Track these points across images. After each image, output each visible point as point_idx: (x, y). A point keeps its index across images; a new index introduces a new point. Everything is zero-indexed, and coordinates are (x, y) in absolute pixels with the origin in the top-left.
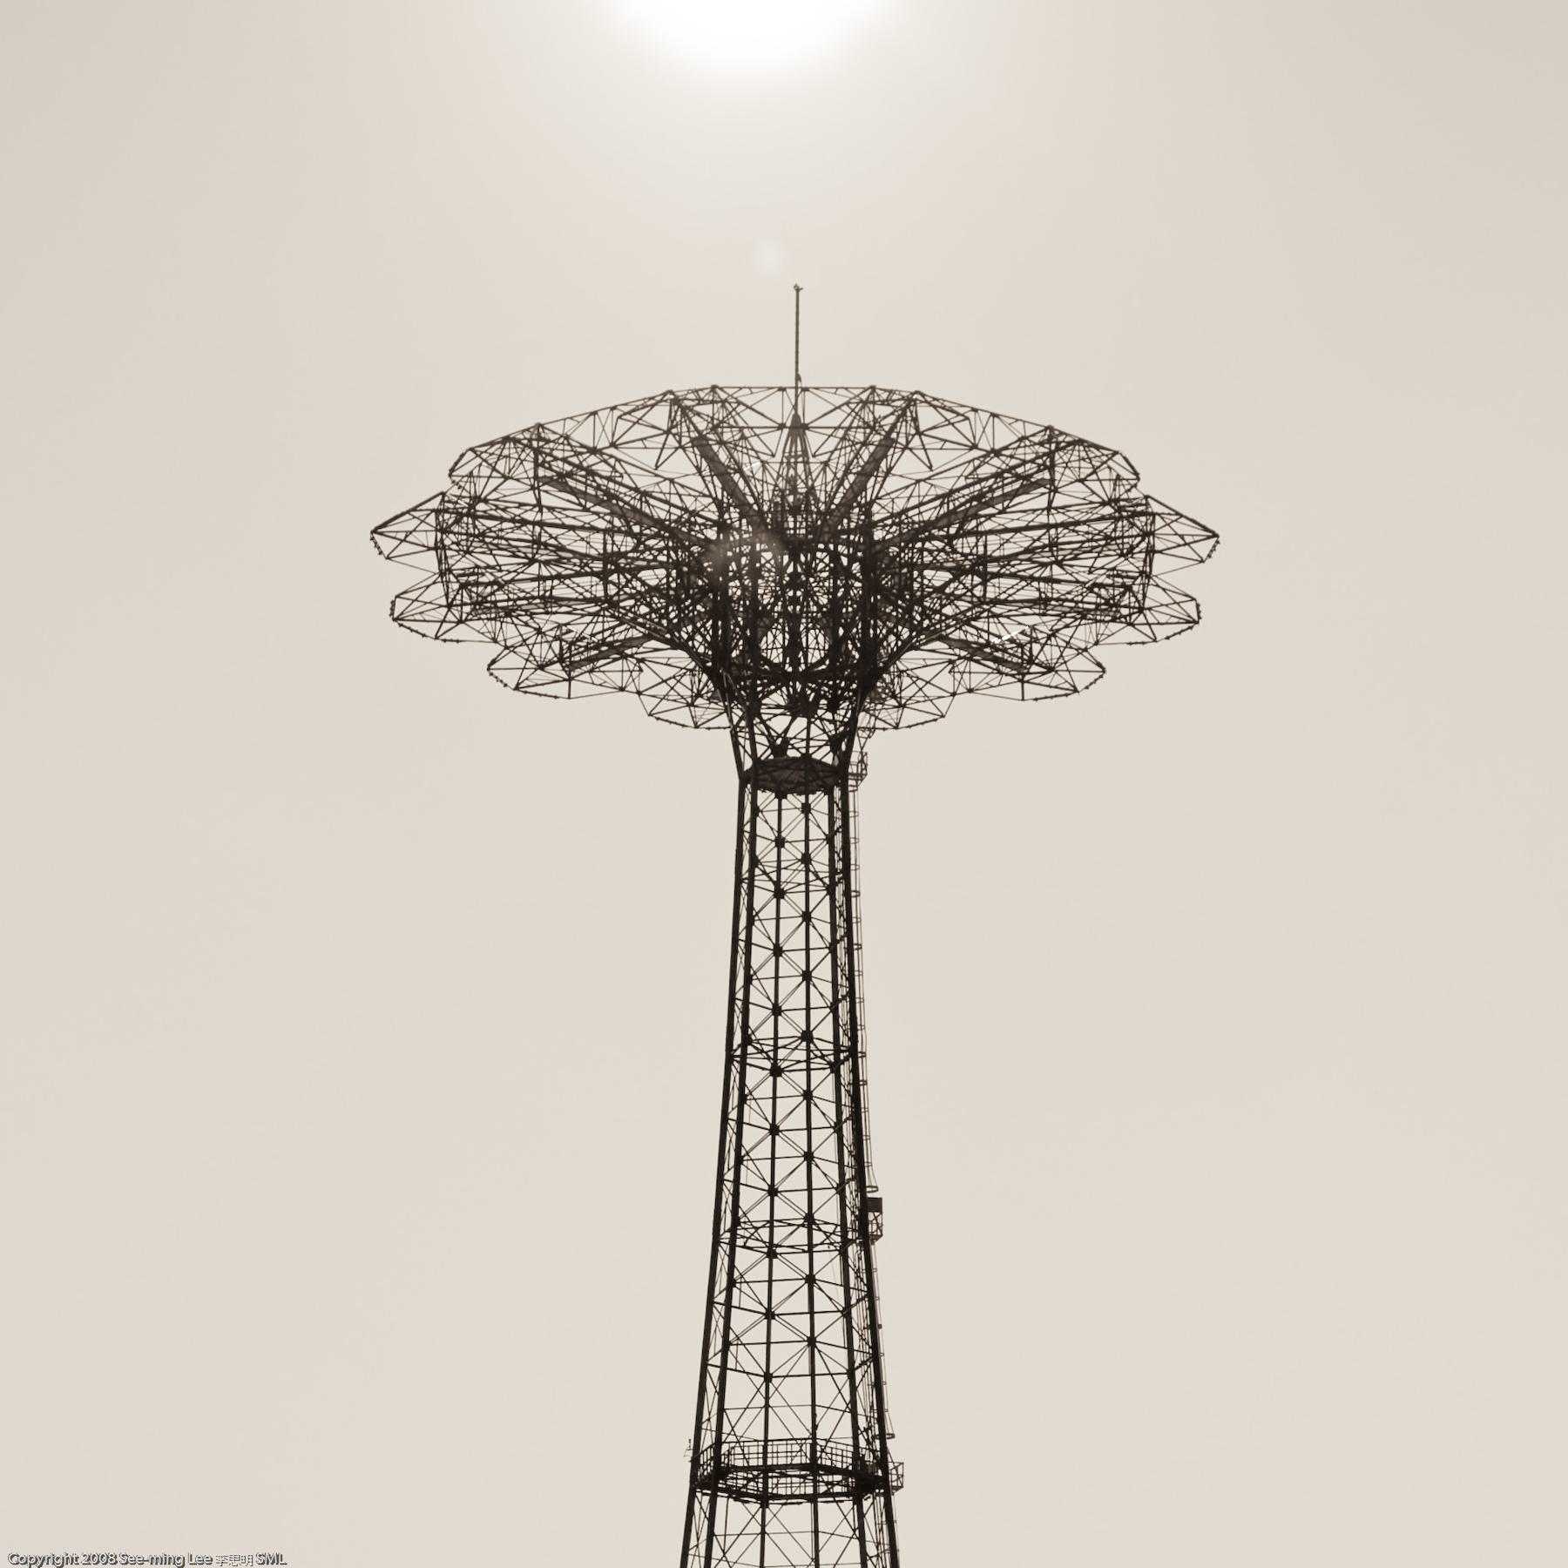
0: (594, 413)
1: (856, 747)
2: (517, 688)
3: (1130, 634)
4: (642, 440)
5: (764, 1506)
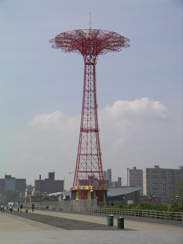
1: (96, 61)
2: (65, 52)
3: (123, 47)
5: (87, 133)
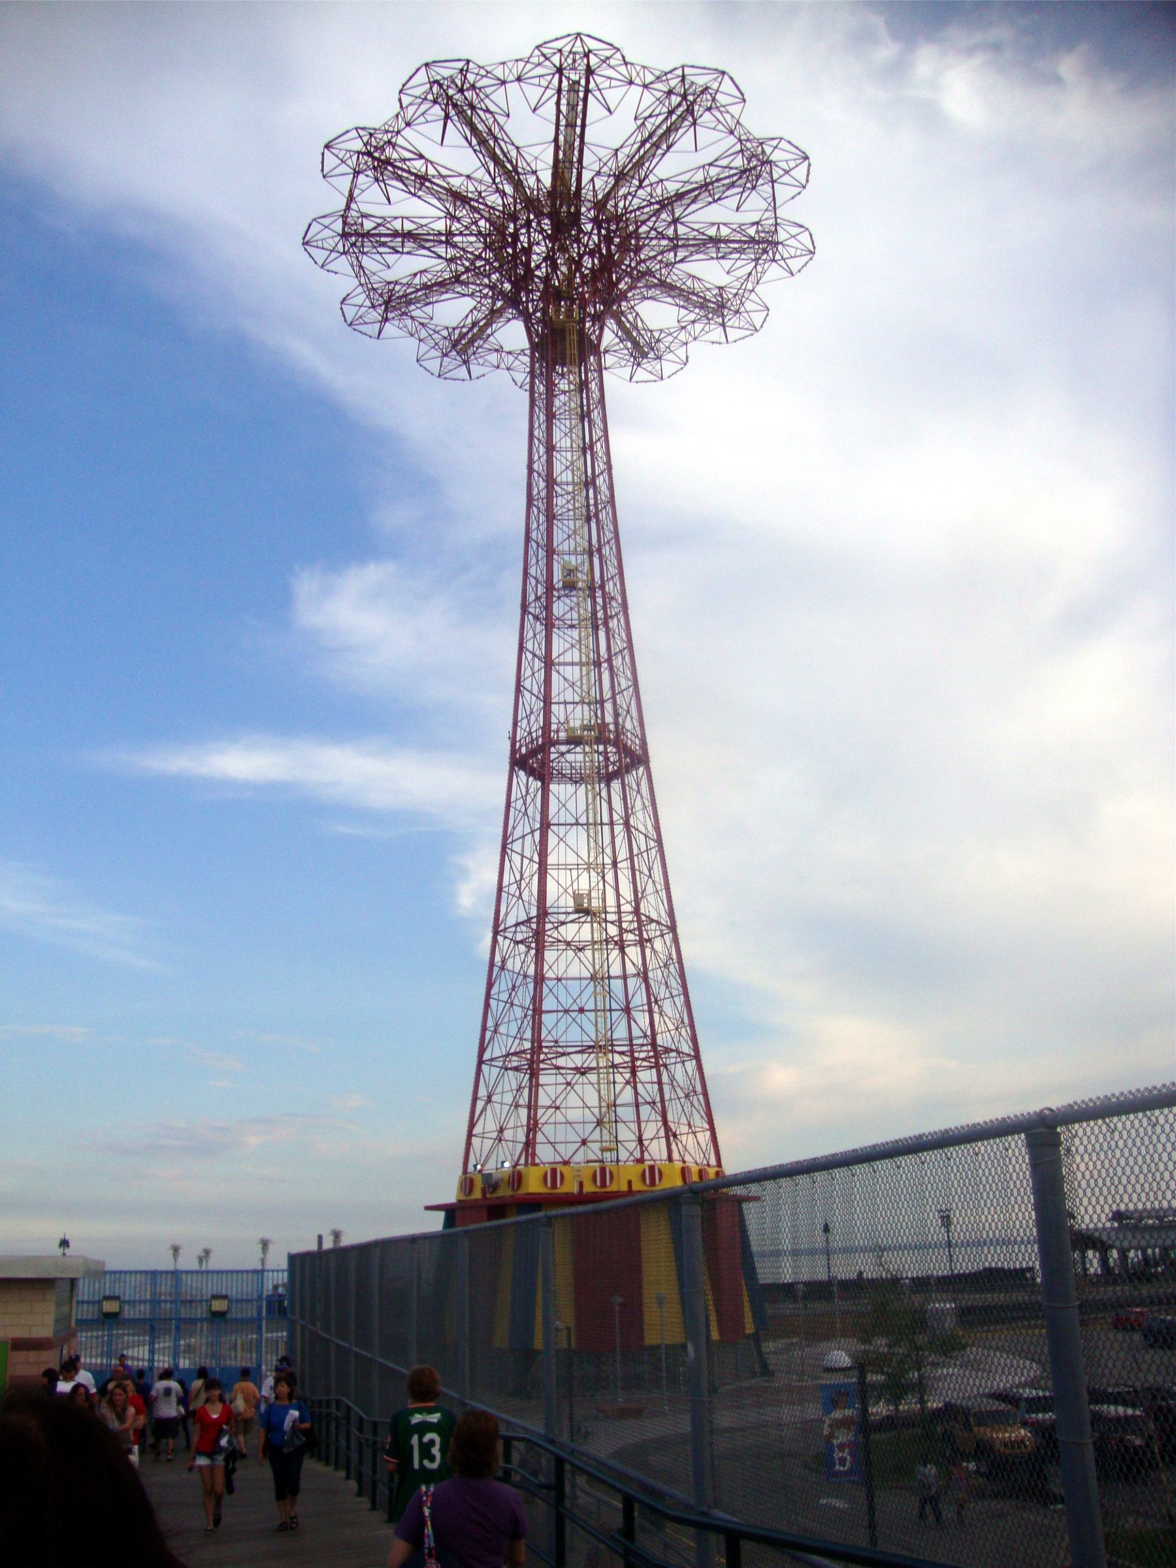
0: (504, 63)
3: (717, 333)
4: (539, 76)
